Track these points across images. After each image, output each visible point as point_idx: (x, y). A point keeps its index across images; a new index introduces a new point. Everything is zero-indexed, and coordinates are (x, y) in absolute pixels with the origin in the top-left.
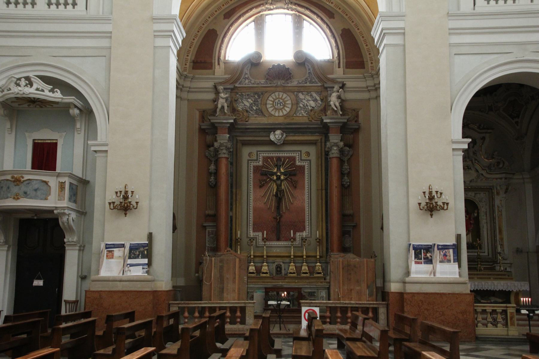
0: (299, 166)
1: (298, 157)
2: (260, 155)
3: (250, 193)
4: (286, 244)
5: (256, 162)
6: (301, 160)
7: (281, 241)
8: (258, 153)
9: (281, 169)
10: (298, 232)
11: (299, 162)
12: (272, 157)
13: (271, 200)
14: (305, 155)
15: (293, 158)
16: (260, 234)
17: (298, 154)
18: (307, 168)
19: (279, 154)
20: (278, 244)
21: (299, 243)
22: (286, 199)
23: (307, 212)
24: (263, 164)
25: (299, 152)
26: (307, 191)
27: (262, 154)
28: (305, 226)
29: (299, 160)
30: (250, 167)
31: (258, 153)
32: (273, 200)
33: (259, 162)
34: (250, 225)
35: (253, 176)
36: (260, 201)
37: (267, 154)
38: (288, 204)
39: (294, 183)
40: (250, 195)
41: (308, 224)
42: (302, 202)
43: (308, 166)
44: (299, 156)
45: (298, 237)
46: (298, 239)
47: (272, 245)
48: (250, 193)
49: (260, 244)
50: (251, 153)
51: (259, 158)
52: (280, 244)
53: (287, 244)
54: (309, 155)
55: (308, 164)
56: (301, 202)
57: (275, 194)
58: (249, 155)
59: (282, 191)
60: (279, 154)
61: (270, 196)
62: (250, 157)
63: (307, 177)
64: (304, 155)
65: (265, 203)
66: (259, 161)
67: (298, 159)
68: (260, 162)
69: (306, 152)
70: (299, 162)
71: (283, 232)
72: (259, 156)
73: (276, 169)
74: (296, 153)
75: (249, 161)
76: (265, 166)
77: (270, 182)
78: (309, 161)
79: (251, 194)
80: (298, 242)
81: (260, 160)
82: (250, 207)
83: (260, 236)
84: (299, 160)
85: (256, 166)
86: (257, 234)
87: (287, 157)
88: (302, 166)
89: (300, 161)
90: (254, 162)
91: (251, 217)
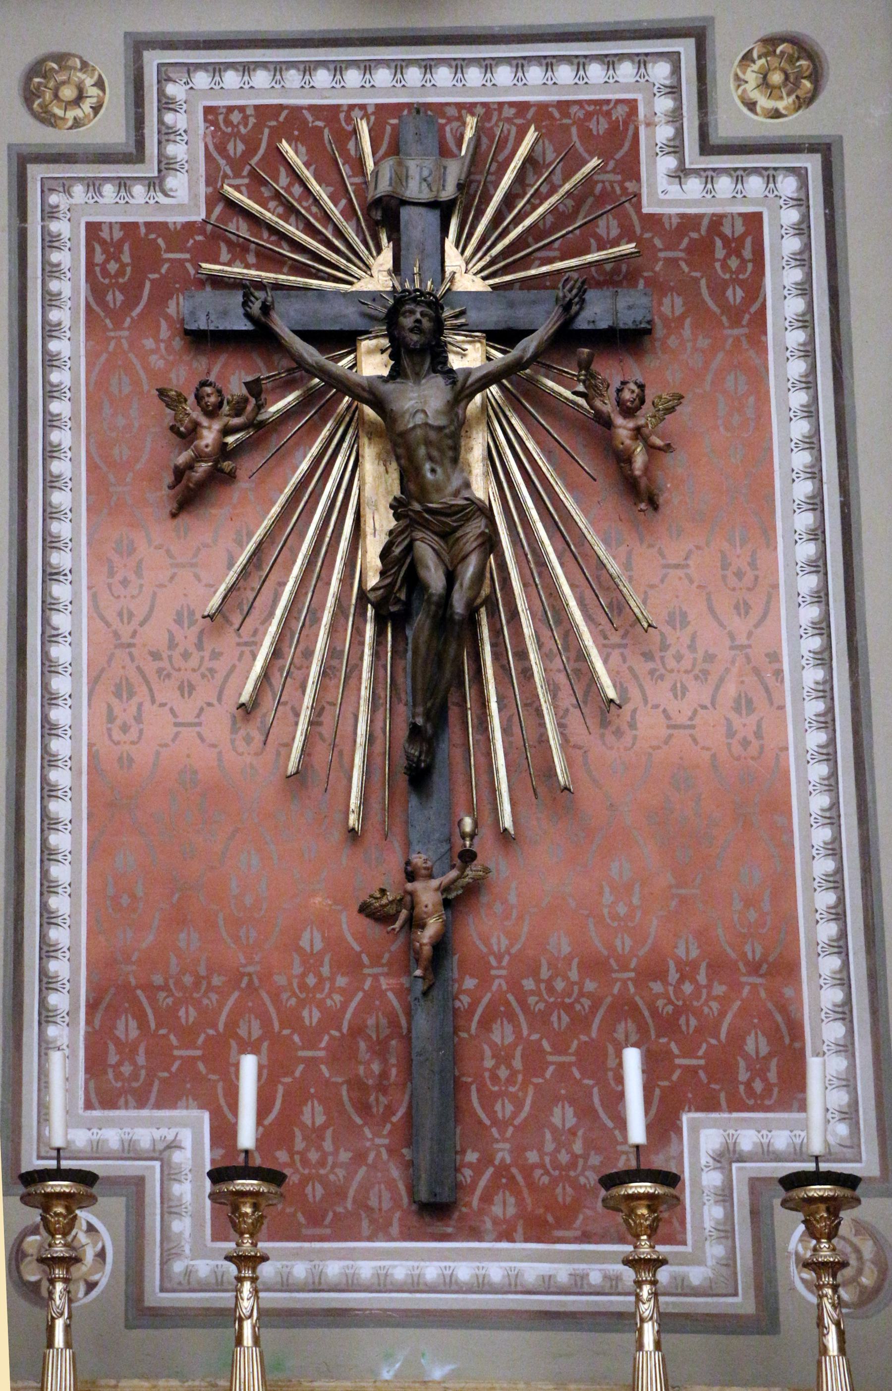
0: (689, 222)
1: (665, 104)
2: (171, 89)
3: (50, 575)
4: (548, 1286)
5: (123, 184)
6: (706, 147)
7: (476, 1234)
8: (153, 59)
9: (454, 259)
10: (709, 1105)
11: (681, 174)
12: (330, 113)
13: (326, 673)
14: (764, 83)
15: (600, 126)
16: (186, 1137)
17: (660, 71)
18: (793, 244)
19: (413, 75)
20: (431, 1271)
21: (729, 1262)
22: (522, 655)
23: (822, 835)
24: (217, 198)
25: (686, 48)
26: (808, 550)
27: (201, 80)
28: (796, 1030)
29: (676, 147)
30: (50, 242)
31: (153, 59)
32: (354, 669)
33: (155, 184)
34: (46, 1016)
35: (92, 357)
36: (187, 689)
37: (261, 78)
38: (561, 726)
39: (623, 427)
40: (49, 605)
41: (832, 996)
42: (744, 704)
43: (802, 229)
44: (674, 90)
45: (712, 1179)
46: (714, 1213)
47: (350, 1285)
48: (50, 575)
49: (190, 1284)
50: (61, 58)
51: (166, 133)
52: (464, 1272)
53: (562, 1272)
54: (816, 76)
55: (801, 202)
56: (731, 689)
57: (373, 580)
58: (29, 95)
59: (477, 527)
60: (413, 75)
61: (314, 617)
62: (47, 119)
63: (797, 368)
64: (751, 76)
65: (247, 710)
66: (166, 165)
67: (665, 132)
68: (176, 182)
69: (771, 42)
70: (681, 174)
71: (504, 1109)
72: (166, 104)
73: (386, 258)
74: (641, 60)
75: (36, 173)
76: (240, 228)
77: (313, 429)
78: (812, 163)
79: (61, 591)
80: (715, 1251)
81: (176, 150)
82: (49, 760)
83: (182, 1158)
84: (676, 147)
85: (129, 228)
86: (145, 1137)
87: (522, 107)
88: (717, 221)
89: (692, 157)
90: (94, 185)
91: (59, 903)
